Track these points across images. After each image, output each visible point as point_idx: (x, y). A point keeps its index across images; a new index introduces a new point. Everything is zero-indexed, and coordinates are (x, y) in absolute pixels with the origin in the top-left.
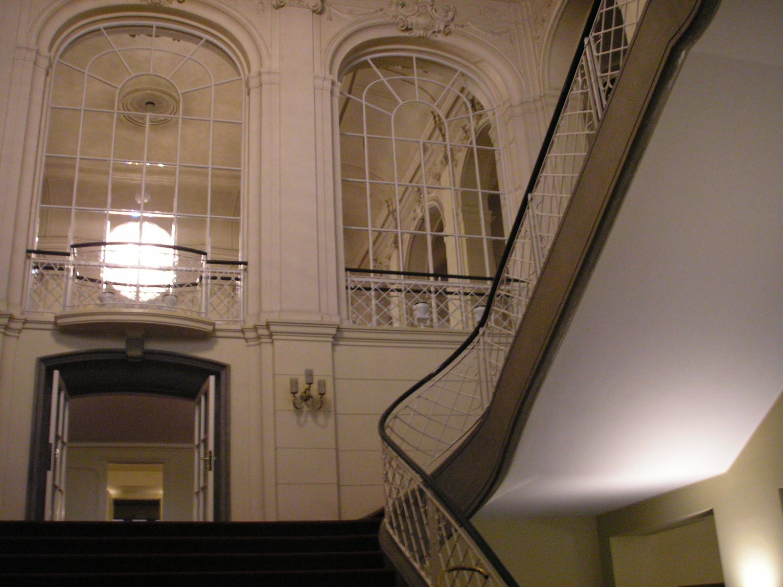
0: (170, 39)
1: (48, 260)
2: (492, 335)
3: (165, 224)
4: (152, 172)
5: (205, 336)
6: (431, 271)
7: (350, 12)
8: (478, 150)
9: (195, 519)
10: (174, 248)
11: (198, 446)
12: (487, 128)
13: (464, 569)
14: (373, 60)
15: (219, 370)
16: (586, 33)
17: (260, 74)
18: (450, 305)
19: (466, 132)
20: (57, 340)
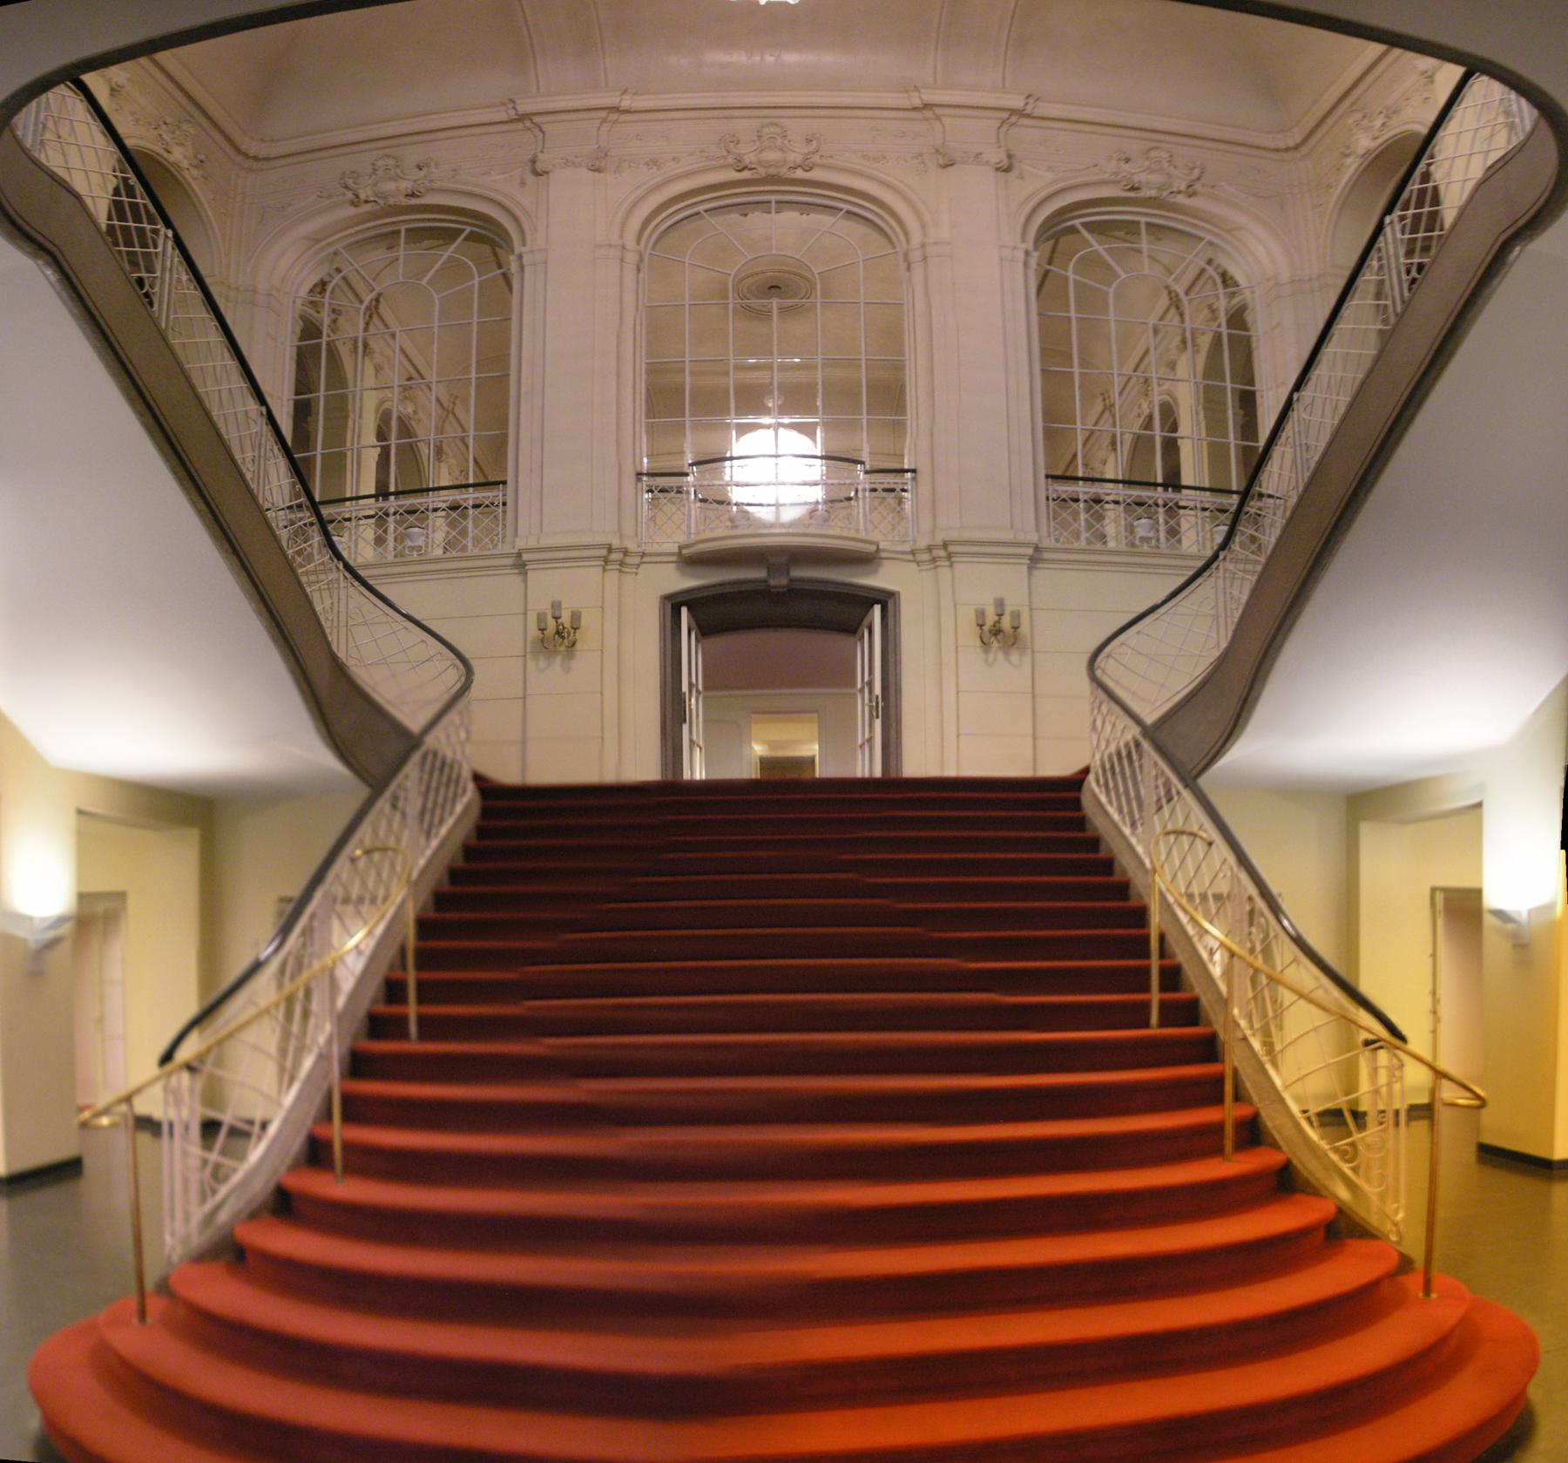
0: (796, 214)
1: (663, 482)
2: (1237, 561)
3: (807, 430)
4: (783, 368)
5: (866, 560)
6: (1160, 480)
7: (1050, 169)
8: (1230, 335)
9: (859, 775)
10: (822, 458)
11: (862, 690)
12: (1242, 309)
13: (1183, 833)
14: (1083, 224)
15: (886, 599)
16: (1389, 210)
17: (923, 246)
18: (1183, 521)
19: (1213, 311)
20: (684, 574)
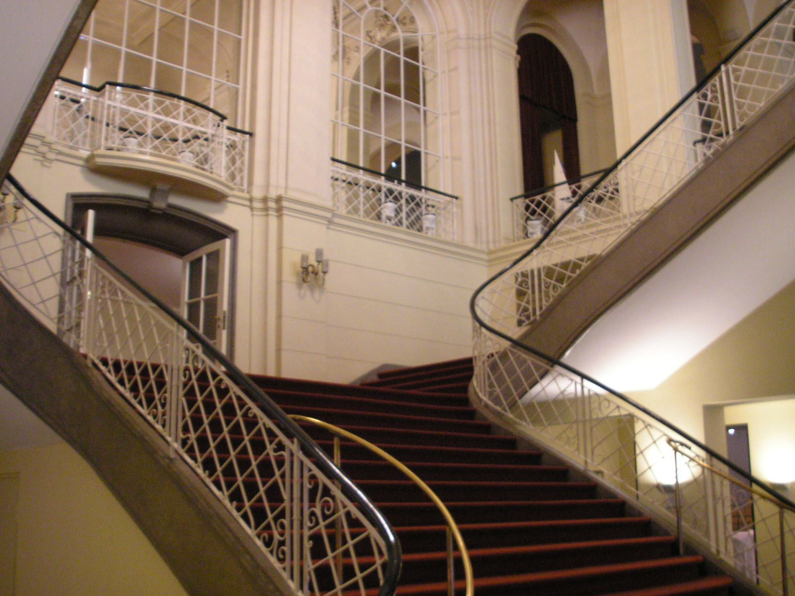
5: (216, 197)
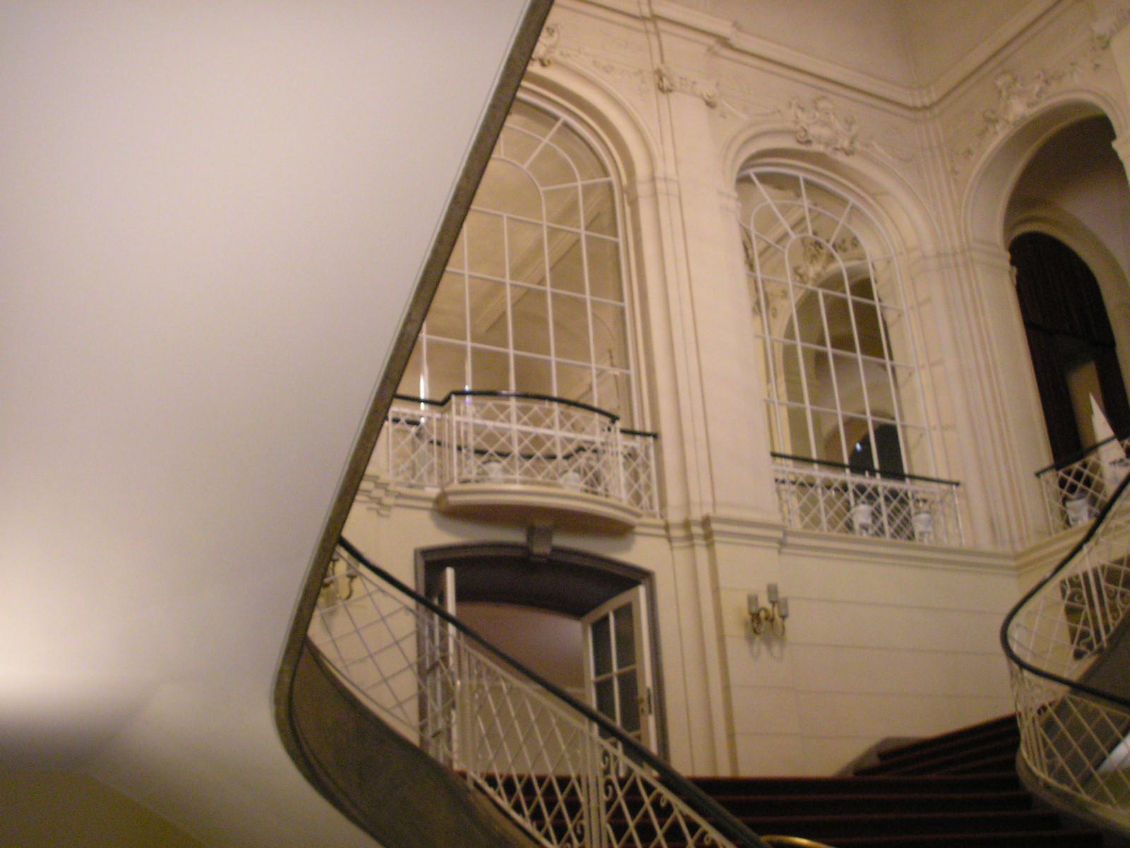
5: (618, 530)
